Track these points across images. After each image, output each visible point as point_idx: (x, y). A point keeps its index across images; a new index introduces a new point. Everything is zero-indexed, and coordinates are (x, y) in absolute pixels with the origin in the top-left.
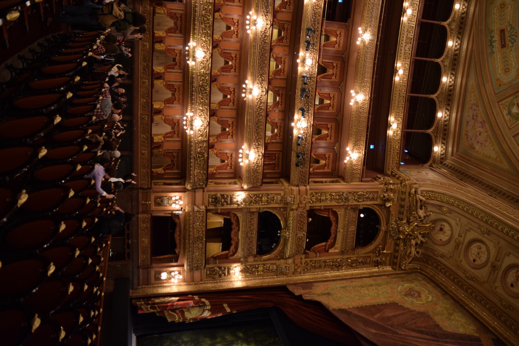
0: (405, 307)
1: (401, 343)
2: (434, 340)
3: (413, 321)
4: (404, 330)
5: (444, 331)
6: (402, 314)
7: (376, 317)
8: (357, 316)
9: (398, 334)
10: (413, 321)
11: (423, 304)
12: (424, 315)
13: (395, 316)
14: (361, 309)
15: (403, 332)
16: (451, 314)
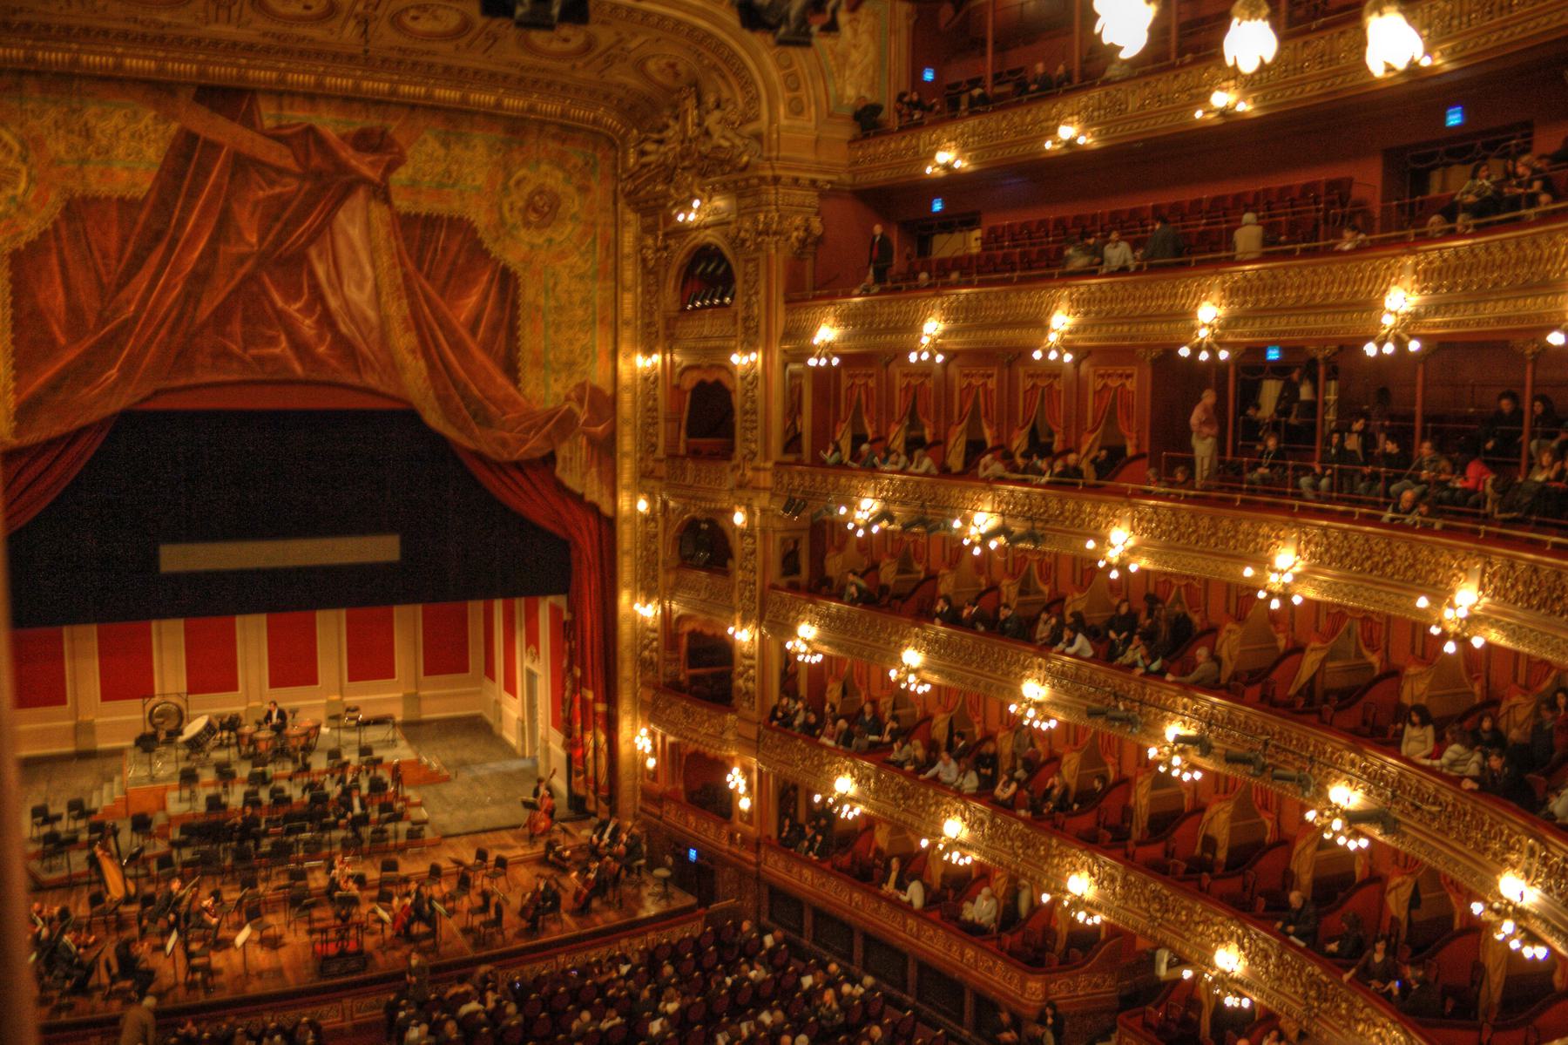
0: (34, 235)
1: (164, 331)
2: (170, 249)
3: (97, 254)
4: (123, 295)
5: (146, 198)
6: (63, 265)
7: (62, 340)
8: (54, 386)
9: (135, 319)
10: (97, 254)
11: (29, 174)
12: (77, 209)
13: (68, 288)
14: (23, 363)
15: (129, 302)
16: (87, 134)
